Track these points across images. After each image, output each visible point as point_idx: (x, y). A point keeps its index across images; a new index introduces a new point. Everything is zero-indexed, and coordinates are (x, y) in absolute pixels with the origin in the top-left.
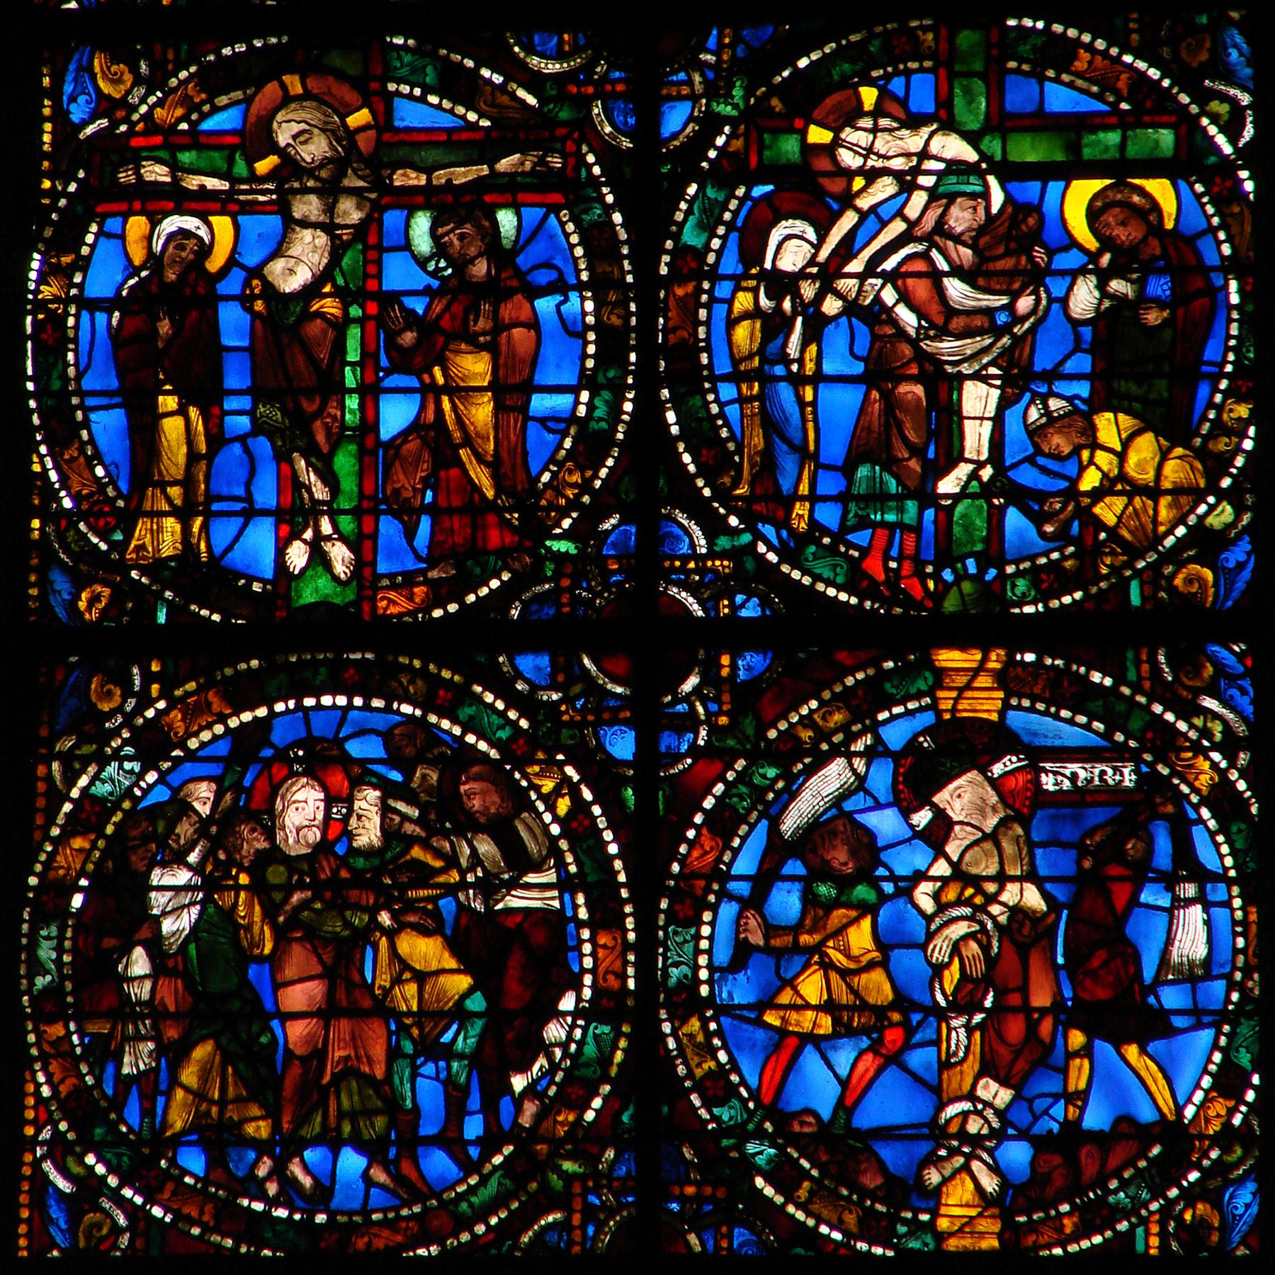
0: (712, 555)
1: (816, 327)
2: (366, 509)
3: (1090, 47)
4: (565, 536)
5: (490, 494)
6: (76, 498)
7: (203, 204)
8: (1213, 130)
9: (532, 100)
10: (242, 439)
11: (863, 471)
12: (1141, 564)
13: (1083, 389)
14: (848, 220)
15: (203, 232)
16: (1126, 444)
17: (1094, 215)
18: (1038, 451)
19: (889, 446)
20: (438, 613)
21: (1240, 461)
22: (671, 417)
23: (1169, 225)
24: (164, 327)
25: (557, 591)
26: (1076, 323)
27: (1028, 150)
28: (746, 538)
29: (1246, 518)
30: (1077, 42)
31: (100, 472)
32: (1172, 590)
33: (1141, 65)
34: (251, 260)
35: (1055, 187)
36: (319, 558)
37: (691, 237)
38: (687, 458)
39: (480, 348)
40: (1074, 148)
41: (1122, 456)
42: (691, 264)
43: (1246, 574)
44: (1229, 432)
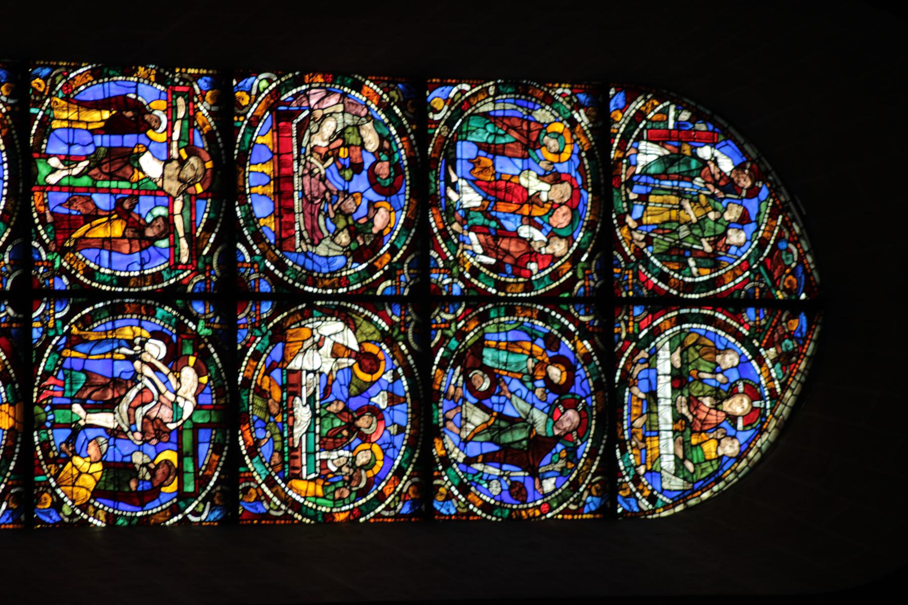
0: (55, 320)
1: (131, 359)
2: (71, 189)
3: (219, 460)
4: (61, 264)
5: (74, 236)
6: (73, 79)
7: (170, 129)
8: (193, 505)
9: (205, 252)
10: (93, 142)
11: (83, 377)
12: (51, 480)
13: (110, 458)
14: (165, 370)
15: (160, 130)
16: (91, 474)
17: (167, 462)
18: (90, 441)
19: (91, 386)
20: (35, 215)
21: (85, 517)
22: (101, 305)
23: (163, 489)
24: (129, 114)
25: (42, 261)
26: (131, 455)
27: (187, 437)
28: (60, 332)
29: (66, 520)
30: (221, 456)
31: (82, 88)
32: (42, 493)
33: (214, 479)
34: (152, 146)
35: (175, 447)
36: (54, 170)
37: (160, 312)
38: (87, 310)
39: (124, 232)
40: (187, 455)
41: (87, 473)
42: (151, 312)
43: (47, 520)
44: (95, 512)
